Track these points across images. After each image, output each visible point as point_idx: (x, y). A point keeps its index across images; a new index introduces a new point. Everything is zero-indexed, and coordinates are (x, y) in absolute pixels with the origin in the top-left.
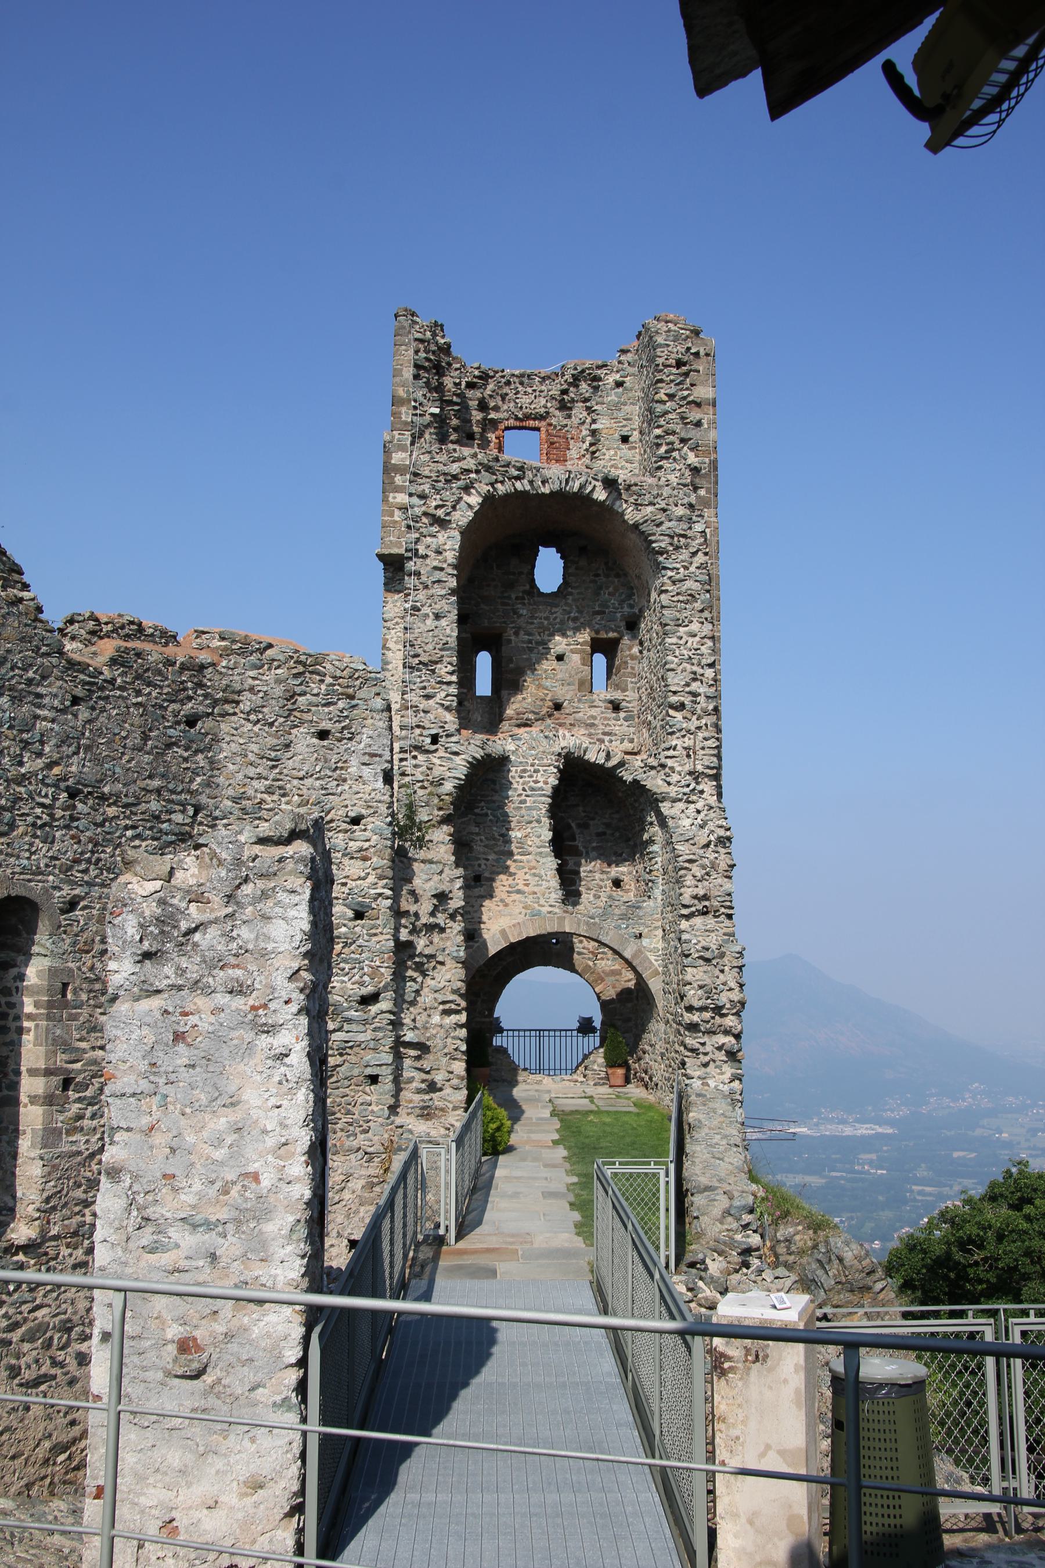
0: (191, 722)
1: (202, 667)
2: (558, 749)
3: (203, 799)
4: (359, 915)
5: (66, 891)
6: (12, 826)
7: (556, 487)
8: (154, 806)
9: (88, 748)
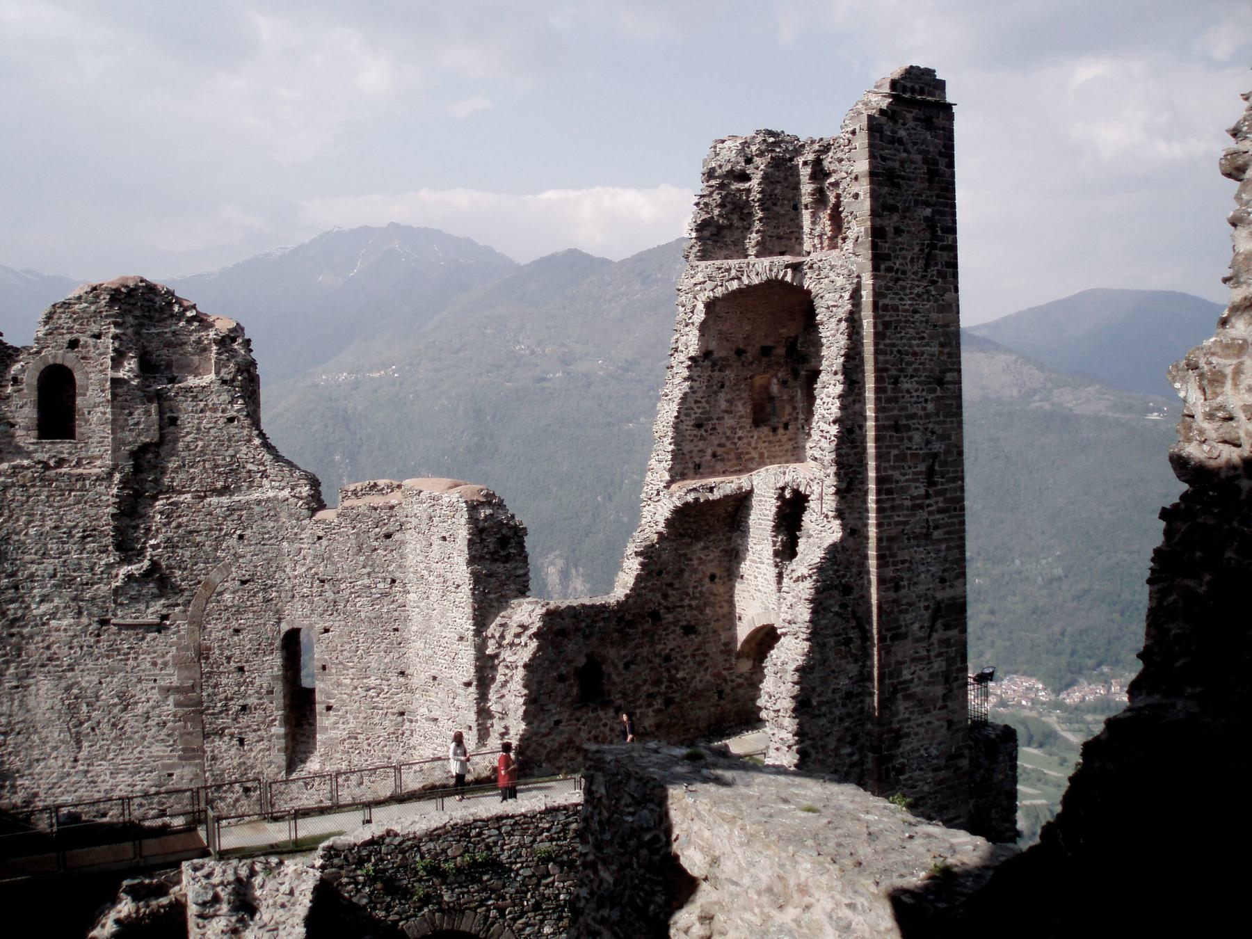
0: (388, 536)
1: (392, 508)
2: (781, 484)
3: (397, 575)
4: (461, 638)
5: (321, 626)
6: (293, 597)
7: (764, 278)
8: (366, 581)
9: (328, 559)
